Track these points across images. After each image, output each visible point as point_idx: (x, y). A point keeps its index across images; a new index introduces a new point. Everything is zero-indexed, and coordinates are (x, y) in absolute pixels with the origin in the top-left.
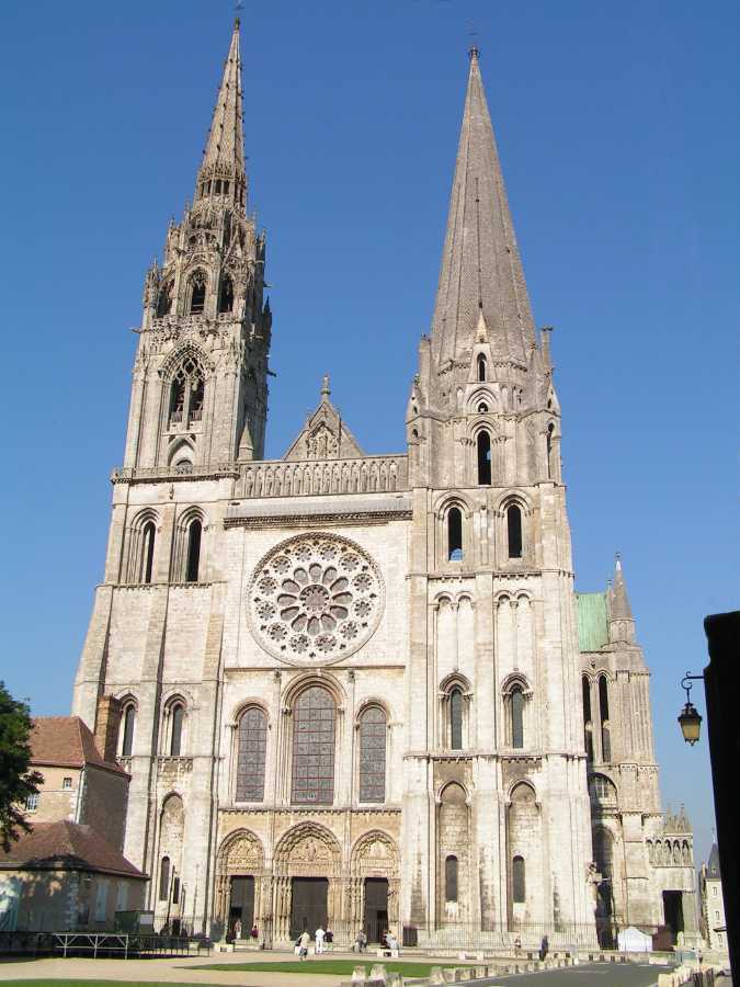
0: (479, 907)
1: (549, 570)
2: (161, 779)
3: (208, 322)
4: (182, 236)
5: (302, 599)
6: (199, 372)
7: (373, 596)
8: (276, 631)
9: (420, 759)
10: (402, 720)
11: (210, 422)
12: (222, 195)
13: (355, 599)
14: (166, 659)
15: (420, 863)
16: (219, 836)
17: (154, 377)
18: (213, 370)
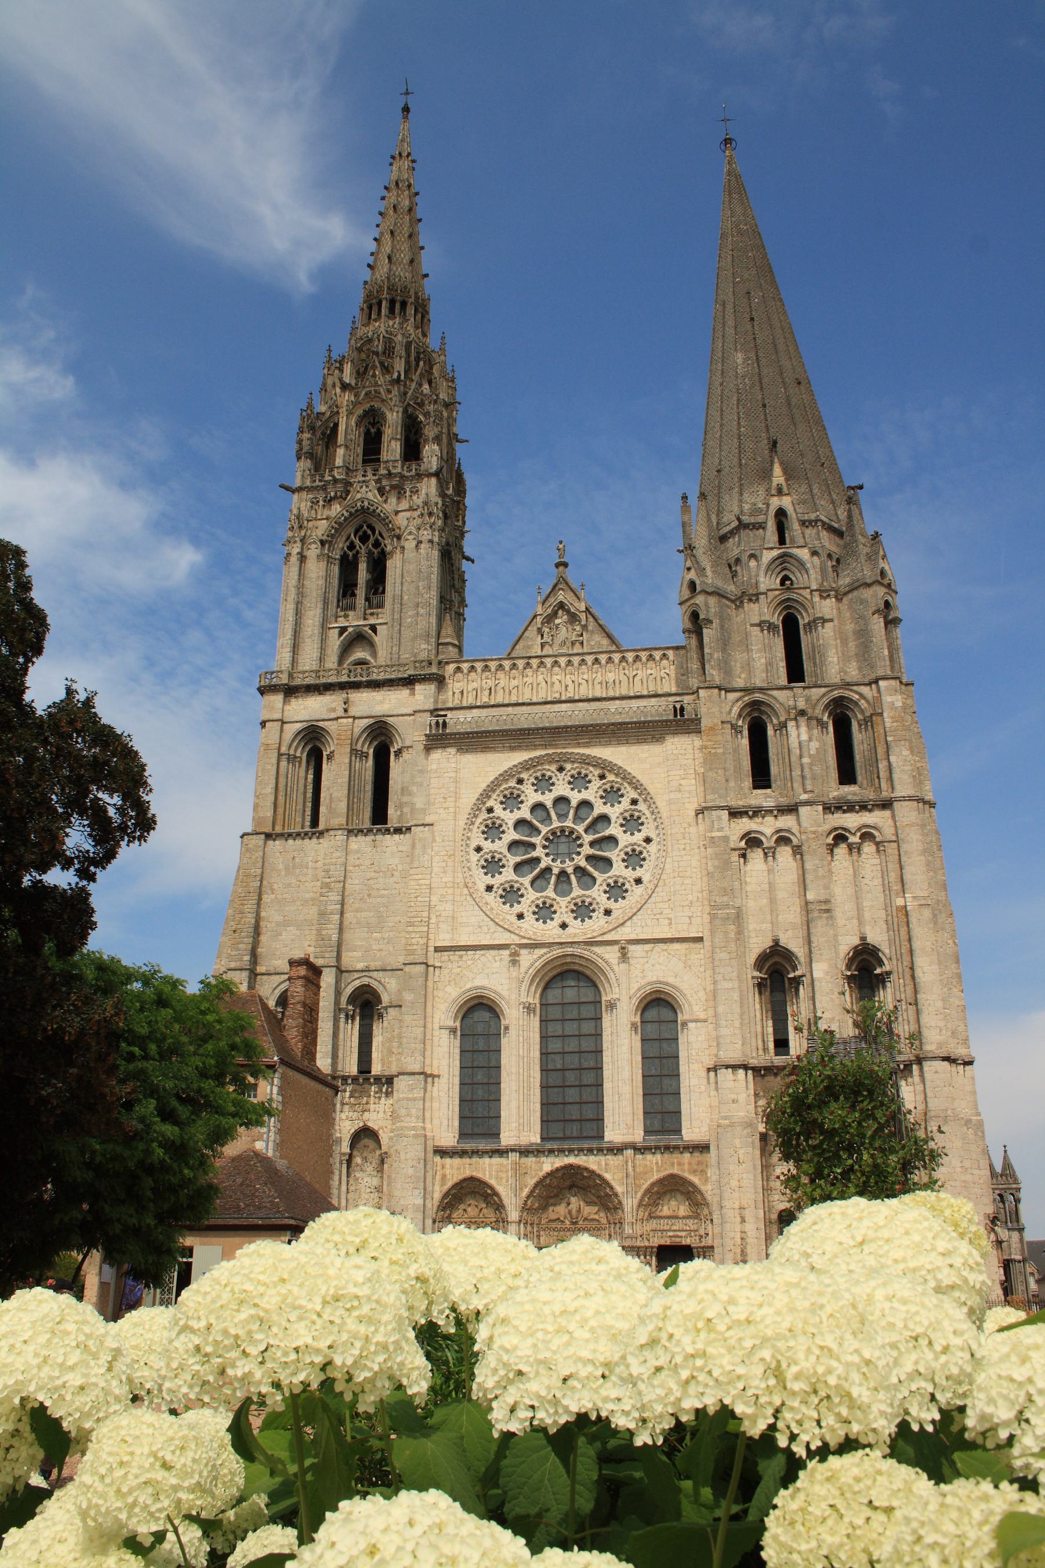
1: (904, 799)
2: (346, 1107)
3: (390, 474)
4: (348, 368)
5: (545, 847)
6: (377, 544)
7: (648, 840)
8: (511, 895)
9: (734, 1067)
10: (702, 1016)
11: (397, 607)
12: (397, 320)
13: (621, 845)
14: (346, 936)
16: (437, 1188)
17: (313, 551)
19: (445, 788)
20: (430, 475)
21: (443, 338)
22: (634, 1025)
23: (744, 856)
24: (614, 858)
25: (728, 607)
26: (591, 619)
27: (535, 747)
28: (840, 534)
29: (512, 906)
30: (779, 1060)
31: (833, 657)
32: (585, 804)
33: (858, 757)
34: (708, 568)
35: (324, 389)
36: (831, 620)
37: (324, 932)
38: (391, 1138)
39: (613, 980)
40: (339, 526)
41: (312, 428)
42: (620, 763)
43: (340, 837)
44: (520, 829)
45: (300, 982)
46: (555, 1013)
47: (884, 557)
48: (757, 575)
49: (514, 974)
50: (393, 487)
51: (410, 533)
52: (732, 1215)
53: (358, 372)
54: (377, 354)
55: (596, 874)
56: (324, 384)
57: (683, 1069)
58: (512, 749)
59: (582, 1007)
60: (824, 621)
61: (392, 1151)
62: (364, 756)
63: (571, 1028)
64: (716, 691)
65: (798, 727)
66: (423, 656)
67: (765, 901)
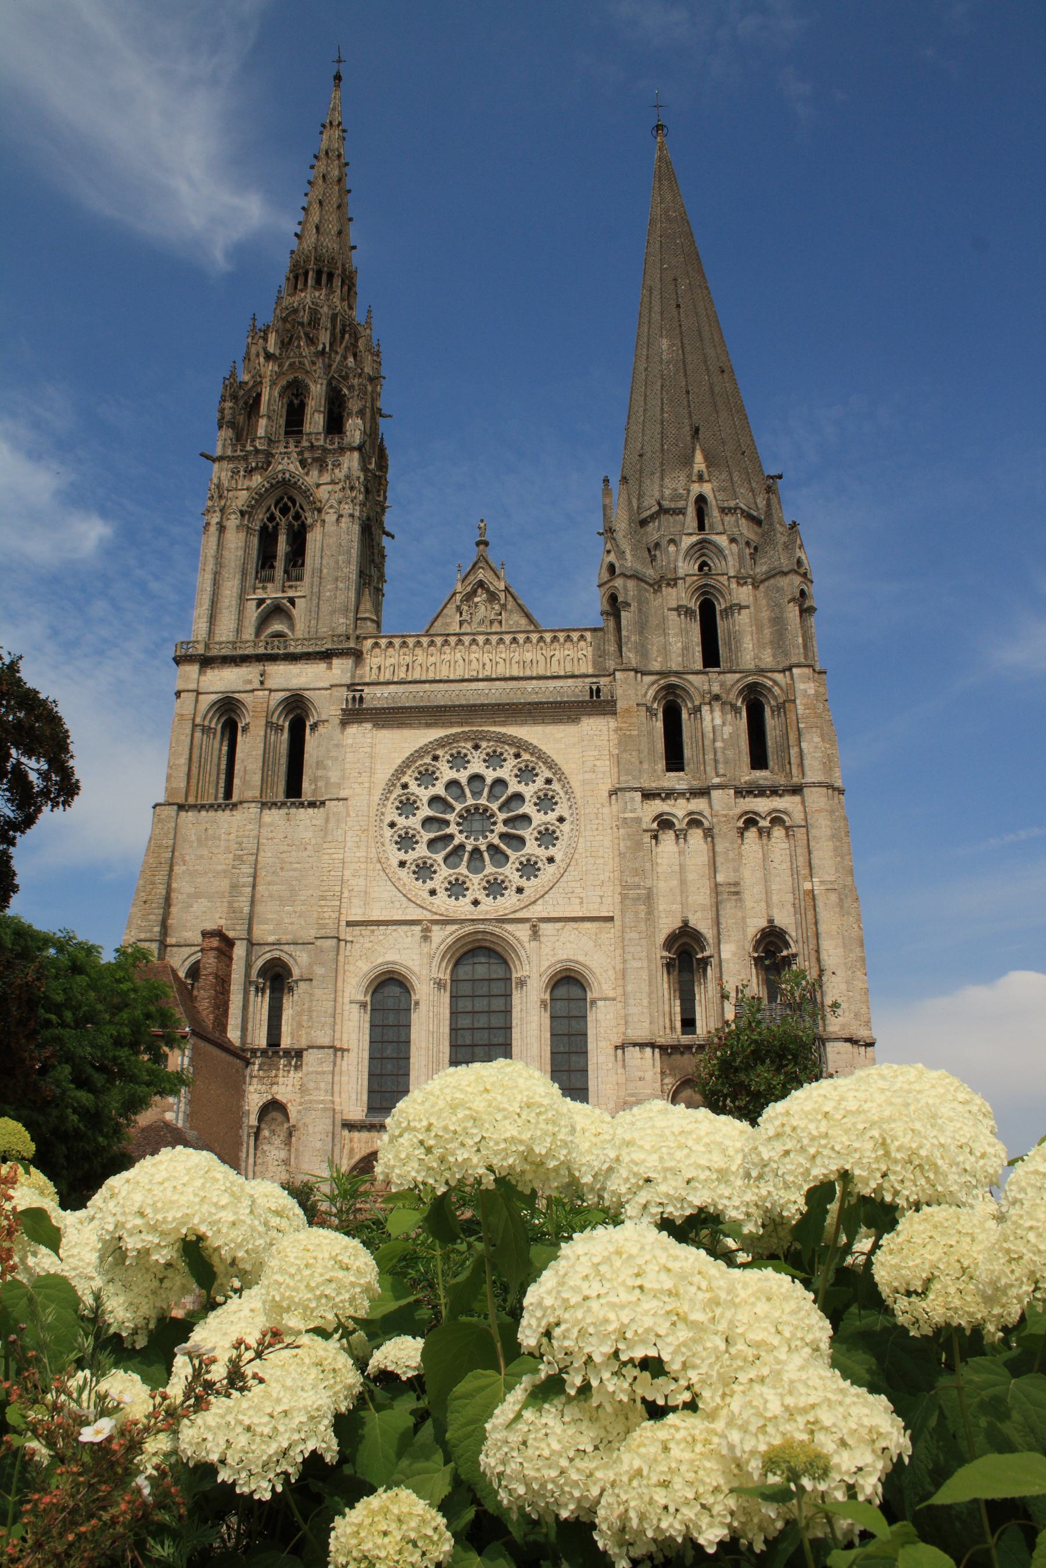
1: (814, 785)
2: (255, 1080)
3: (312, 447)
4: (272, 338)
5: (458, 824)
6: (297, 516)
7: (561, 820)
8: (424, 871)
9: (642, 1045)
10: (611, 994)
11: (316, 580)
12: (324, 292)
13: (534, 824)
14: (259, 908)
16: (345, 1161)
17: (233, 522)
19: (360, 763)
20: (352, 449)
21: (369, 312)
22: (543, 1003)
23: (656, 837)
24: (527, 837)
25: (646, 590)
26: (510, 599)
27: (452, 724)
28: (758, 522)
29: (424, 882)
30: (686, 1039)
31: (749, 644)
32: (500, 782)
33: (770, 742)
34: (628, 552)
35: (247, 358)
36: (747, 607)
37: (236, 905)
38: (299, 1112)
39: (524, 958)
40: (259, 498)
41: (234, 397)
42: (535, 742)
43: (254, 809)
44: (434, 805)
45: (212, 954)
46: (465, 989)
47: (801, 546)
48: (676, 560)
49: (426, 950)
50: (315, 460)
51: (331, 507)
53: (282, 342)
54: (302, 324)
55: (509, 852)
56: (248, 353)
57: (591, 1046)
58: (428, 725)
59: (493, 983)
60: (741, 607)
61: (300, 1124)
62: (279, 729)
63: (481, 1004)
64: (632, 673)
65: (712, 711)
66: (341, 630)
67: (675, 883)
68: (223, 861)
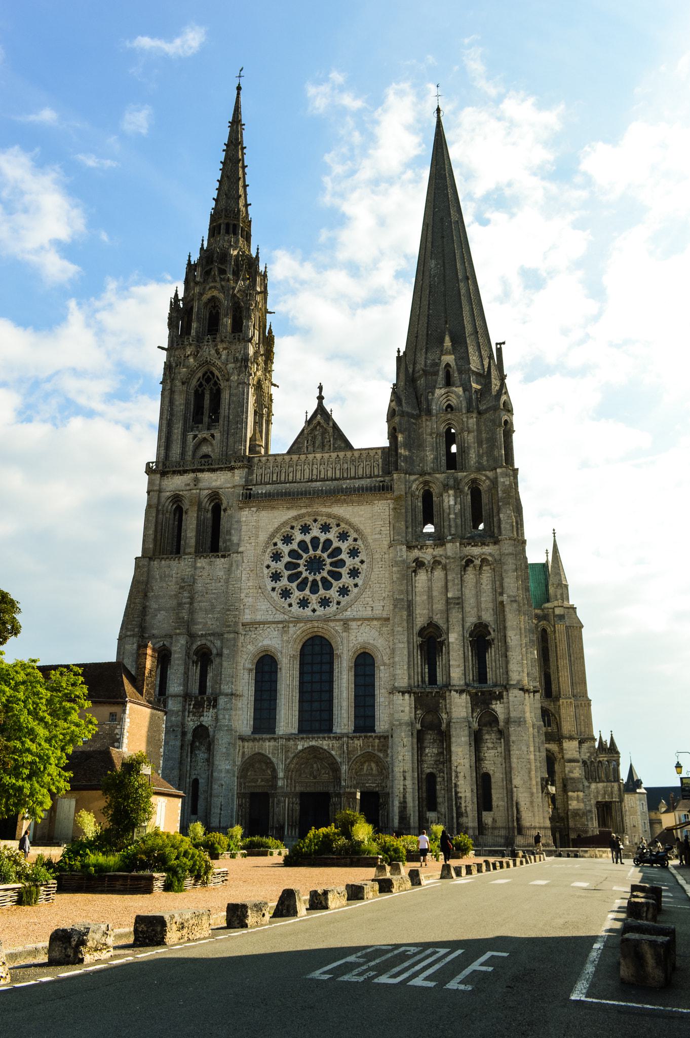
0: (455, 815)
6: (216, 384)
7: (362, 562)
8: (286, 594)
9: (403, 693)
13: (347, 564)
15: (405, 779)
18: (228, 380)
25: (415, 424)
37: (181, 615)
40: (192, 373)
52: (398, 775)
55: (333, 581)
57: (377, 692)
58: (288, 509)
64: (403, 475)
68: (173, 588)
